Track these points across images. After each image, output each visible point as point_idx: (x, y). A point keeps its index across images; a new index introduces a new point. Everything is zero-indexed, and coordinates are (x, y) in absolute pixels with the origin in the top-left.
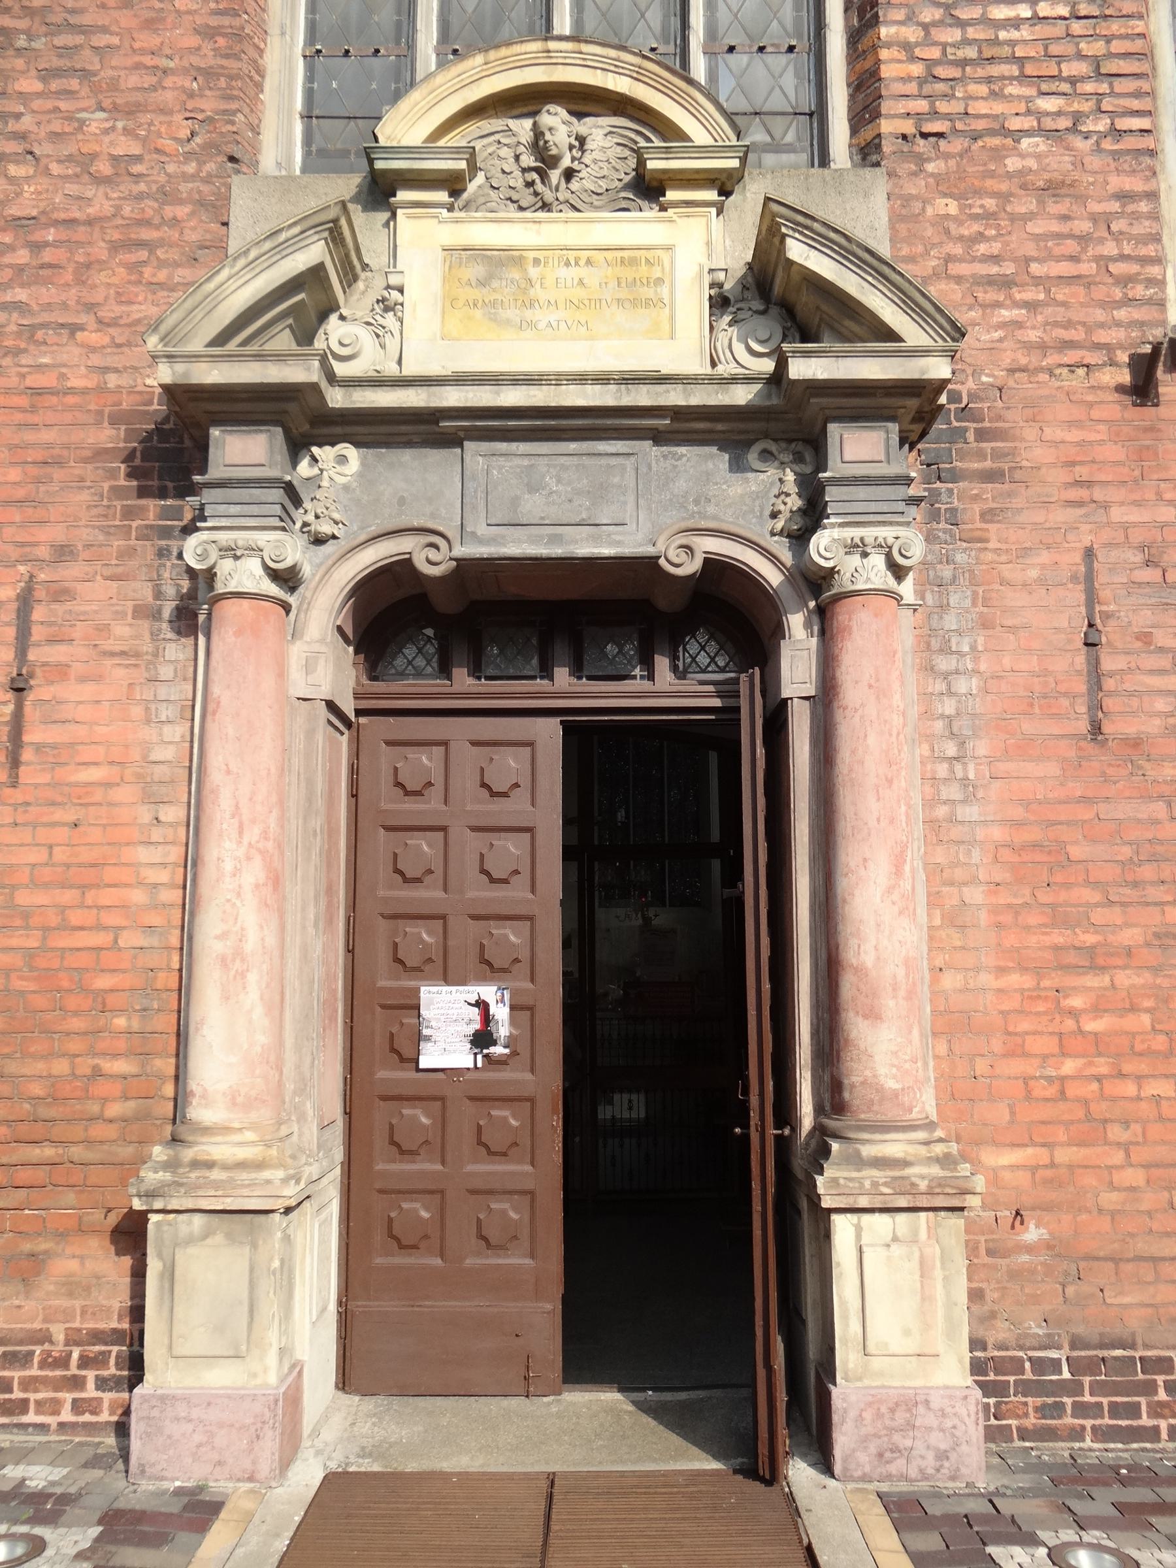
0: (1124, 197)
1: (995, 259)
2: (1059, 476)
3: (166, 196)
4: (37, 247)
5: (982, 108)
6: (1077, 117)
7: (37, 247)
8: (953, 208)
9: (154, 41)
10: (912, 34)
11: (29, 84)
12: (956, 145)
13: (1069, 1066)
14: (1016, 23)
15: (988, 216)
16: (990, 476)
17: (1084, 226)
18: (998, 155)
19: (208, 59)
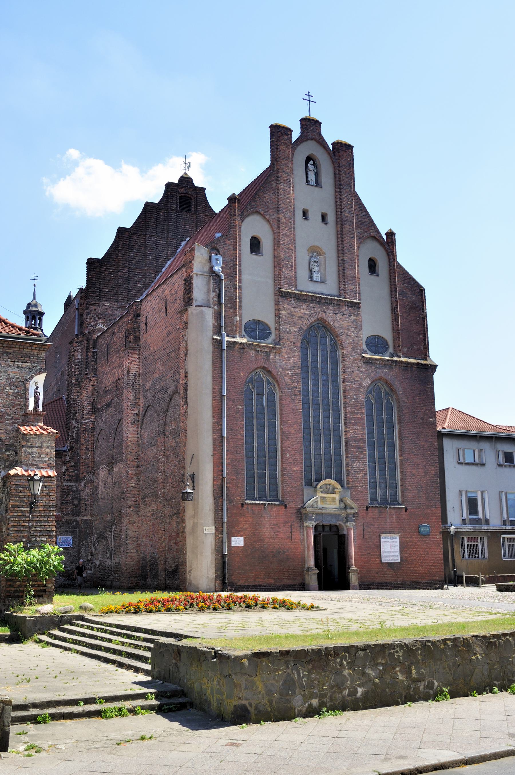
0: (366, 493)
2: (361, 517)
3: (299, 490)
9: (296, 475)
10: (351, 477)
12: (354, 488)
18: (357, 489)
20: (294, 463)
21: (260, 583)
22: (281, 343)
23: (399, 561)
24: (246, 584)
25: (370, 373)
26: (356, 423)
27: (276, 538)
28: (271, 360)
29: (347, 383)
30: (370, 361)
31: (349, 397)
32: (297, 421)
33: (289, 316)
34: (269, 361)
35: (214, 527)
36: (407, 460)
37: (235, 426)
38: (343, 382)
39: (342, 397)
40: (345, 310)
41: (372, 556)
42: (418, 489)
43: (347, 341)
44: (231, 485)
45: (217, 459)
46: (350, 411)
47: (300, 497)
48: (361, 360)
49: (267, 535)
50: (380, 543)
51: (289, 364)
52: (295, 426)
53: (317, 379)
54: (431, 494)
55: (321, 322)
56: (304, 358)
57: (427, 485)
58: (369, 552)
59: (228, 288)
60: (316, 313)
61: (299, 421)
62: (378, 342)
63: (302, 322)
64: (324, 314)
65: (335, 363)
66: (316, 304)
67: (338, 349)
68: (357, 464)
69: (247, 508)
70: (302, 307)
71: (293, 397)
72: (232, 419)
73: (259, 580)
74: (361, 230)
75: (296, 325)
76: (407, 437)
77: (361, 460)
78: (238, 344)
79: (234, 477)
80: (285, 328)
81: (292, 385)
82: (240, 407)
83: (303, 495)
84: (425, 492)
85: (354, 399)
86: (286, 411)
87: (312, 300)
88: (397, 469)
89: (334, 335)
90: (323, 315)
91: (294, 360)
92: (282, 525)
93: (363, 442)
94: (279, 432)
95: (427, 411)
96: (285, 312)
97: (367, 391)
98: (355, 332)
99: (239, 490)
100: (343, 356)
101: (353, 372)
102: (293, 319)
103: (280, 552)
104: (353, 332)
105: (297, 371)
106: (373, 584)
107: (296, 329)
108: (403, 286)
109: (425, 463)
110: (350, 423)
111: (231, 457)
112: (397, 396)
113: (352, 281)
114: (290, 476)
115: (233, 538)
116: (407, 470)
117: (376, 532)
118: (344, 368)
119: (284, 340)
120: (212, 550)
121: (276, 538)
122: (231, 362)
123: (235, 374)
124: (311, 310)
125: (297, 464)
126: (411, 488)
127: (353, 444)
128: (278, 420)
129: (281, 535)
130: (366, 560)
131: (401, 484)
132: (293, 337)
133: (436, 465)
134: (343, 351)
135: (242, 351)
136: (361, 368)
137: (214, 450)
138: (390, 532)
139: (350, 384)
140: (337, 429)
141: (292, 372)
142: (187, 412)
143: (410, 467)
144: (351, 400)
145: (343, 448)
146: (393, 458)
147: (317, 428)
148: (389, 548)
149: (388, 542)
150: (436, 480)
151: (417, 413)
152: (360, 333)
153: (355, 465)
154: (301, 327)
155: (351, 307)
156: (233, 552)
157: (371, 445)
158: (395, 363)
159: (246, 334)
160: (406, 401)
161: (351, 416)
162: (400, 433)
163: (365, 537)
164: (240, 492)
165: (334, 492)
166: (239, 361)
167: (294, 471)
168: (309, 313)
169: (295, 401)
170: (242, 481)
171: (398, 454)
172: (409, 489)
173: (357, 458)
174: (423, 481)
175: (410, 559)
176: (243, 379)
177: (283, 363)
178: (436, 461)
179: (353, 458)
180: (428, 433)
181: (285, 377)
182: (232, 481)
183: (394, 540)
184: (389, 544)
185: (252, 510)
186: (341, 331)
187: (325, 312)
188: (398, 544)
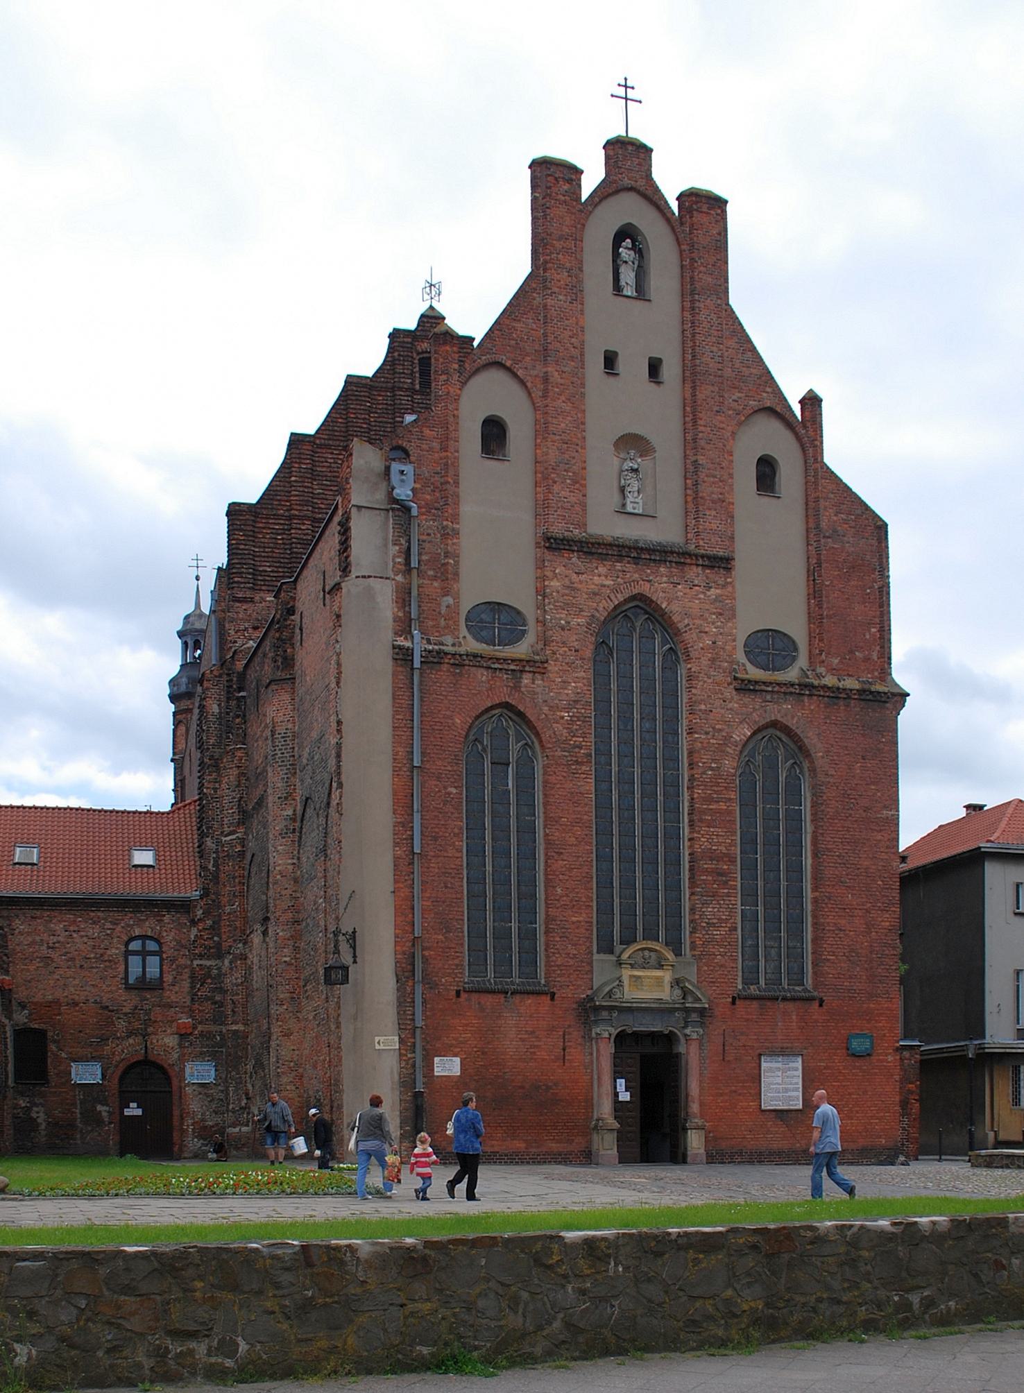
3: (582, 962)
7: (561, 970)
10: (701, 936)
11: (558, 939)
15: (712, 970)
16: (710, 1016)
17: (726, 973)
18: (714, 959)
19: (587, 935)
20: (574, 906)
21: (496, 1149)
22: (547, 652)
25: (751, 713)
26: (715, 820)
28: (523, 689)
29: (696, 736)
30: (752, 687)
31: (700, 764)
32: (581, 819)
33: (567, 592)
34: (520, 691)
35: (397, 1038)
38: (688, 734)
39: (686, 765)
40: (696, 574)
41: (741, 1098)
43: (698, 643)
44: (432, 953)
45: (402, 900)
46: (703, 795)
47: (585, 976)
48: (729, 684)
49: (511, 1053)
50: (760, 1070)
51: (564, 697)
52: (575, 828)
53: (629, 727)
54: (880, 970)
55: (641, 604)
56: (600, 679)
57: (871, 952)
59: (429, 535)
60: (630, 582)
61: (585, 817)
62: (773, 644)
63: (595, 604)
64: (648, 585)
65: (672, 694)
66: (629, 563)
67: (679, 664)
68: (714, 908)
70: (596, 571)
71: (574, 767)
72: (435, 816)
73: (493, 1142)
75: (581, 610)
76: (829, 850)
78: (449, 657)
79: (440, 937)
80: (556, 618)
81: (572, 742)
82: (454, 791)
83: (591, 972)
84: (866, 966)
85: (712, 769)
86: (557, 796)
88: (806, 919)
89: (669, 631)
90: (645, 589)
92: (545, 1033)
93: (730, 861)
94: (542, 841)
95: (879, 794)
96: (558, 584)
97: (741, 752)
98: (719, 624)
99: (450, 962)
100: (690, 678)
101: (711, 711)
102: (574, 597)
103: (540, 1086)
104: (713, 623)
105: (583, 711)
106: (740, 1153)
109: (869, 905)
110: (701, 820)
112: (812, 762)
114: (564, 933)
115: (437, 1059)
116: (827, 920)
118: (692, 703)
119: (554, 644)
121: (532, 1059)
123: (442, 721)
124: (618, 577)
125: (580, 909)
127: (706, 866)
128: (539, 817)
131: (812, 949)
132: (575, 637)
133: (894, 909)
134: (689, 666)
135: (458, 671)
136: (731, 702)
137: (396, 882)
139: (703, 737)
140: (673, 835)
141: (571, 714)
142: (341, 803)
143: (834, 914)
144: (704, 773)
145: (685, 875)
146: (797, 895)
147: (627, 834)
149: (778, 1069)
150: (892, 940)
151: (854, 799)
152: (730, 624)
153: (709, 909)
154: (593, 616)
155: (712, 567)
156: (438, 1087)
157: (749, 868)
158: (809, 690)
159: (470, 633)
160: (832, 772)
161: (705, 807)
162: (815, 842)
163: (727, 1059)
164: (453, 967)
165: (660, 967)
166: (451, 692)
167: (573, 923)
168: (612, 583)
169: (577, 776)
170: (457, 944)
171: (809, 886)
172: (828, 960)
174: (862, 943)
176: (461, 732)
177: (552, 694)
180: (880, 840)
181: (554, 725)
182: (435, 945)
183: (791, 1065)
184: (780, 1074)
185: (479, 1003)
186: (686, 621)
187: (649, 581)
188: (800, 1073)
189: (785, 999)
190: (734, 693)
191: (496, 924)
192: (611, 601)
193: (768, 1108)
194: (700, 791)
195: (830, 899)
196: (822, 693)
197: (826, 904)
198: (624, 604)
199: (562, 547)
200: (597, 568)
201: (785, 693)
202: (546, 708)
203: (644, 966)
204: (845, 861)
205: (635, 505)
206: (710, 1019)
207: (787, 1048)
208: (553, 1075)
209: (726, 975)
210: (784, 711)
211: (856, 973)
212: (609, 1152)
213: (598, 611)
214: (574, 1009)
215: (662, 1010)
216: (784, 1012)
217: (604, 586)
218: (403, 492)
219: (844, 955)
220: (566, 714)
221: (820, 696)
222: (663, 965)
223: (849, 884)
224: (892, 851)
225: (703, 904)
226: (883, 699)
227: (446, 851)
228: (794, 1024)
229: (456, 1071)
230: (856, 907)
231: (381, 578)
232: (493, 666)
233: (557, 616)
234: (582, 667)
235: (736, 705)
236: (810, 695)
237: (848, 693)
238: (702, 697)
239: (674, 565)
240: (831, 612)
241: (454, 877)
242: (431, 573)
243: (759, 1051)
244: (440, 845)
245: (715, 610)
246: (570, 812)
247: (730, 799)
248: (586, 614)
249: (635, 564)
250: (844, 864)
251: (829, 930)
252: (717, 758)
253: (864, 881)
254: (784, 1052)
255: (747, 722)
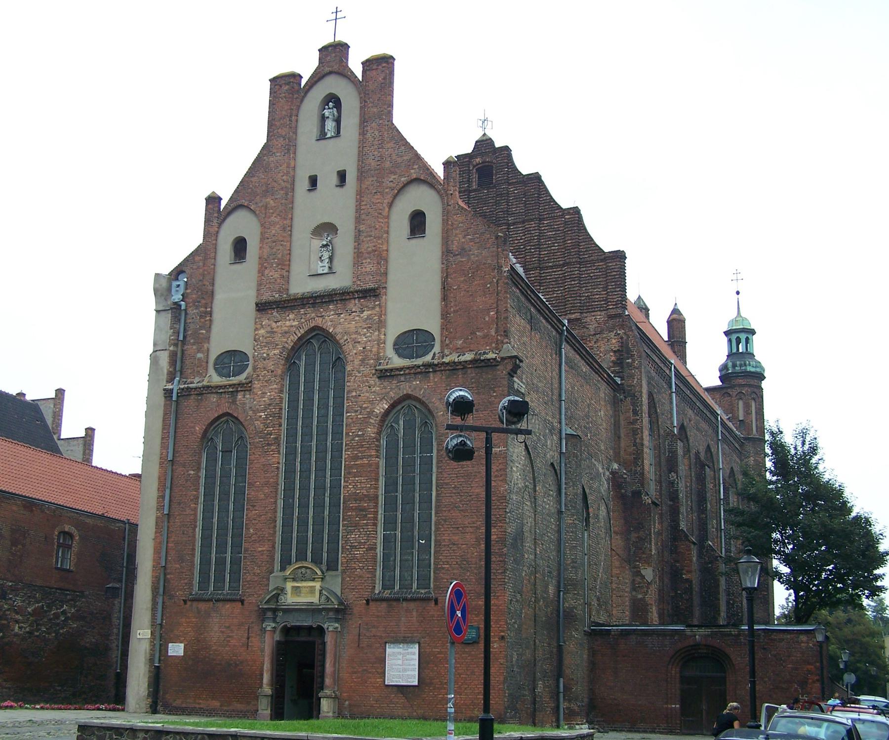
0: (368, 577)
1: (353, 586)
3: (263, 578)
4: (250, 584)
5: (353, 565)
6: (364, 567)
8: (349, 579)
9: (262, 557)
10: (345, 555)
12: (349, 571)
13: (352, 684)
14: (357, 554)
15: (352, 580)
16: (350, 614)
17: (363, 581)
18: (354, 572)
21: (202, 706)
23: (416, 683)
24: (184, 705)
25: (388, 393)
27: (227, 645)
28: (238, 403)
31: (351, 434)
35: (149, 631)
36: (445, 521)
37: (184, 498)
40: (354, 305)
42: (461, 568)
43: (352, 353)
46: (351, 455)
47: (265, 588)
58: (365, 668)
63: (285, 340)
64: (321, 319)
66: (309, 308)
68: (356, 535)
69: (191, 605)
70: (288, 318)
71: (266, 448)
73: (201, 701)
74: (394, 177)
75: (277, 345)
76: (447, 484)
77: (363, 529)
78: (193, 390)
79: (178, 566)
80: (260, 354)
82: (192, 472)
84: (476, 571)
85: (358, 436)
86: (254, 468)
87: (303, 304)
90: (319, 322)
91: (271, 395)
93: (369, 500)
98: (368, 334)
101: (360, 396)
104: (364, 335)
107: (276, 352)
108: (463, 240)
110: (349, 473)
111: (176, 539)
113: (370, 258)
115: (170, 645)
116: (444, 538)
117: (381, 637)
120: (146, 660)
121: (227, 645)
122: (186, 415)
123: (189, 430)
125: (264, 542)
126: (448, 566)
127: (351, 505)
129: (233, 642)
130: (360, 680)
132: (273, 363)
133: (501, 524)
135: (199, 398)
137: (156, 532)
138: (404, 637)
139: (353, 414)
140: (336, 486)
141: (266, 413)
147: (305, 488)
148: (400, 662)
149: (400, 653)
150: (499, 549)
152: (377, 333)
153: (353, 536)
154: (284, 347)
155: (364, 297)
156: (170, 663)
157: (390, 504)
163: (361, 646)
165: (313, 580)
167: (259, 552)
172: (443, 568)
173: (356, 525)
175: (438, 680)
177: (255, 402)
178: (501, 519)
179: (351, 527)
183: (410, 650)
184: (400, 657)
186: (345, 338)
189: (405, 599)
190: (377, 380)
191: (217, 555)
192: (296, 335)
193: (391, 684)
194: (349, 453)
195: (445, 521)
196: (442, 368)
197: (442, 525)
198: (308, 335)
199: (266, 308)
200: (288, 316)
201: (415, 374)
202: (251, 412)
203: (304, 579)
204: (459, 491)
205: (323, 268)
206: (350, 616)
207: (408, 637)
208: (240, 656)
209: (363, 583)
210: (414, 386)
211: (467, 577)
212: (265, 712)
213: (287, 343)
214: (256, 611)
215: (312, 610)
216: (406, 610)
217: (292, 326)
218: (177, 297)
219: (457, 564)
220: (263, 414)
221: (442, 370)
222: (315, 578)
223: (463, 508)
224: (501, 478)
225: (348, 533)
226: (493, 364)
227: (185, 511)
228: (415, 618)
229: (181, 653)
230: (468, 525)
231: (163, 350)
232: (219, 391)
233: (262, 352)
234: (275, 381)
235: (378, 389)
236: (435, 371)
237: (464, 365)
238: (354, 387)
239: (339, 302)
240: (458, 308)
241: (188, 527)
242: (192, 341)
243: (385, 640)
244: (182, 507)
245: (366, 326)
246: (262, 477)
247: (371, 456)
248: (279, 347)
249: (313, 307)
250: (458, 493)
251: (445, 545)
252: (363, 428)
253: (475, 505)
254: (406, 640)
255: (385, 399)
